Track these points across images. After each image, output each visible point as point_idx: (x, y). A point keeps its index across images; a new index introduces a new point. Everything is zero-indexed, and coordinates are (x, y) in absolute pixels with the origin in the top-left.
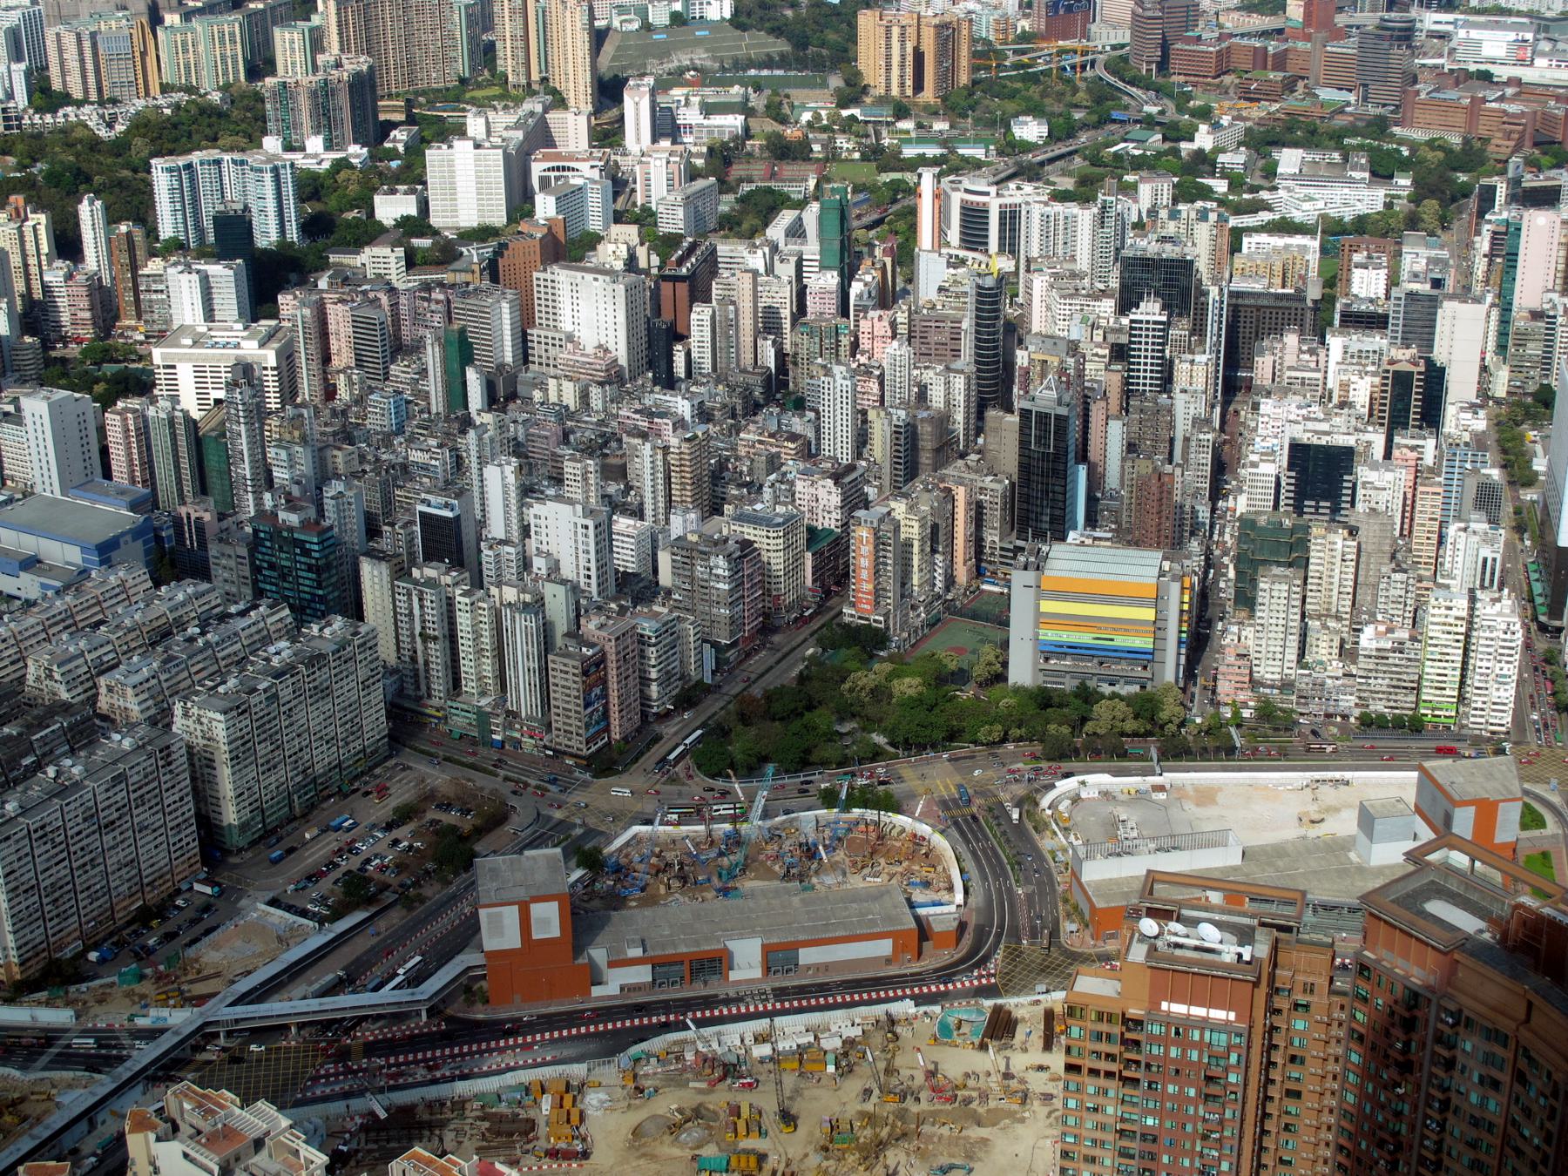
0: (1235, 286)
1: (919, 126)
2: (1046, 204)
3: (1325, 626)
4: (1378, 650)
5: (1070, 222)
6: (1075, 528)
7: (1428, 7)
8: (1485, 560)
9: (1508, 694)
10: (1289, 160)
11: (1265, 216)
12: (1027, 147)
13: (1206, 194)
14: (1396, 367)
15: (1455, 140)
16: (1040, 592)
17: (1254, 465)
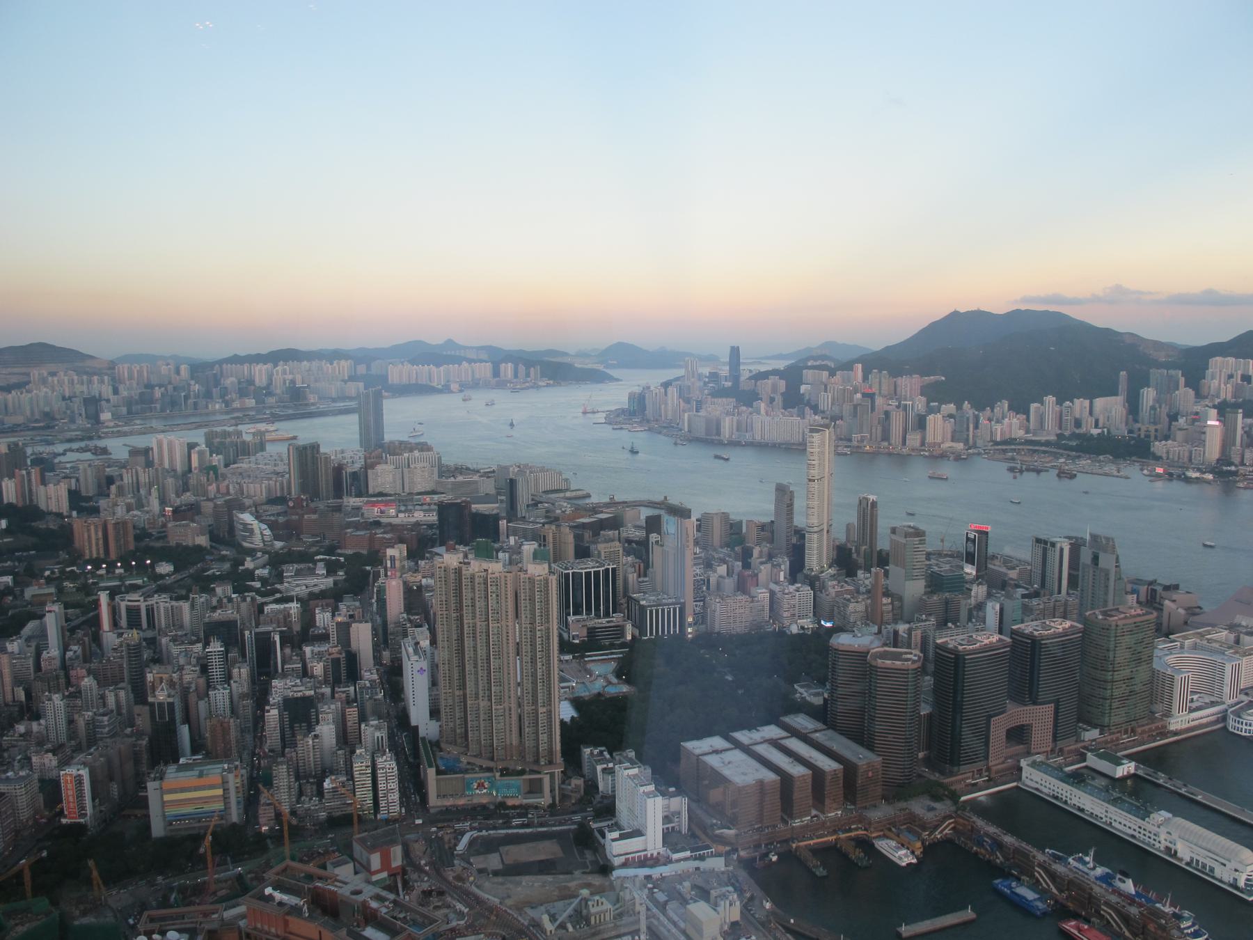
0: (258, 630)
1: (108, 572)
2: (166, 602)
3: (308, 782)
4: (333, 788)
6: (183, 756)
7: (351, 496)
8: (378, 737)
9: (395, 796)
10: (289, 570)
11: (278, 595)
12: (162, 577)
13: (251, 589)
14: (332, 656)
15: (365, 552)
16: (163, 792)
17: (268, 711)
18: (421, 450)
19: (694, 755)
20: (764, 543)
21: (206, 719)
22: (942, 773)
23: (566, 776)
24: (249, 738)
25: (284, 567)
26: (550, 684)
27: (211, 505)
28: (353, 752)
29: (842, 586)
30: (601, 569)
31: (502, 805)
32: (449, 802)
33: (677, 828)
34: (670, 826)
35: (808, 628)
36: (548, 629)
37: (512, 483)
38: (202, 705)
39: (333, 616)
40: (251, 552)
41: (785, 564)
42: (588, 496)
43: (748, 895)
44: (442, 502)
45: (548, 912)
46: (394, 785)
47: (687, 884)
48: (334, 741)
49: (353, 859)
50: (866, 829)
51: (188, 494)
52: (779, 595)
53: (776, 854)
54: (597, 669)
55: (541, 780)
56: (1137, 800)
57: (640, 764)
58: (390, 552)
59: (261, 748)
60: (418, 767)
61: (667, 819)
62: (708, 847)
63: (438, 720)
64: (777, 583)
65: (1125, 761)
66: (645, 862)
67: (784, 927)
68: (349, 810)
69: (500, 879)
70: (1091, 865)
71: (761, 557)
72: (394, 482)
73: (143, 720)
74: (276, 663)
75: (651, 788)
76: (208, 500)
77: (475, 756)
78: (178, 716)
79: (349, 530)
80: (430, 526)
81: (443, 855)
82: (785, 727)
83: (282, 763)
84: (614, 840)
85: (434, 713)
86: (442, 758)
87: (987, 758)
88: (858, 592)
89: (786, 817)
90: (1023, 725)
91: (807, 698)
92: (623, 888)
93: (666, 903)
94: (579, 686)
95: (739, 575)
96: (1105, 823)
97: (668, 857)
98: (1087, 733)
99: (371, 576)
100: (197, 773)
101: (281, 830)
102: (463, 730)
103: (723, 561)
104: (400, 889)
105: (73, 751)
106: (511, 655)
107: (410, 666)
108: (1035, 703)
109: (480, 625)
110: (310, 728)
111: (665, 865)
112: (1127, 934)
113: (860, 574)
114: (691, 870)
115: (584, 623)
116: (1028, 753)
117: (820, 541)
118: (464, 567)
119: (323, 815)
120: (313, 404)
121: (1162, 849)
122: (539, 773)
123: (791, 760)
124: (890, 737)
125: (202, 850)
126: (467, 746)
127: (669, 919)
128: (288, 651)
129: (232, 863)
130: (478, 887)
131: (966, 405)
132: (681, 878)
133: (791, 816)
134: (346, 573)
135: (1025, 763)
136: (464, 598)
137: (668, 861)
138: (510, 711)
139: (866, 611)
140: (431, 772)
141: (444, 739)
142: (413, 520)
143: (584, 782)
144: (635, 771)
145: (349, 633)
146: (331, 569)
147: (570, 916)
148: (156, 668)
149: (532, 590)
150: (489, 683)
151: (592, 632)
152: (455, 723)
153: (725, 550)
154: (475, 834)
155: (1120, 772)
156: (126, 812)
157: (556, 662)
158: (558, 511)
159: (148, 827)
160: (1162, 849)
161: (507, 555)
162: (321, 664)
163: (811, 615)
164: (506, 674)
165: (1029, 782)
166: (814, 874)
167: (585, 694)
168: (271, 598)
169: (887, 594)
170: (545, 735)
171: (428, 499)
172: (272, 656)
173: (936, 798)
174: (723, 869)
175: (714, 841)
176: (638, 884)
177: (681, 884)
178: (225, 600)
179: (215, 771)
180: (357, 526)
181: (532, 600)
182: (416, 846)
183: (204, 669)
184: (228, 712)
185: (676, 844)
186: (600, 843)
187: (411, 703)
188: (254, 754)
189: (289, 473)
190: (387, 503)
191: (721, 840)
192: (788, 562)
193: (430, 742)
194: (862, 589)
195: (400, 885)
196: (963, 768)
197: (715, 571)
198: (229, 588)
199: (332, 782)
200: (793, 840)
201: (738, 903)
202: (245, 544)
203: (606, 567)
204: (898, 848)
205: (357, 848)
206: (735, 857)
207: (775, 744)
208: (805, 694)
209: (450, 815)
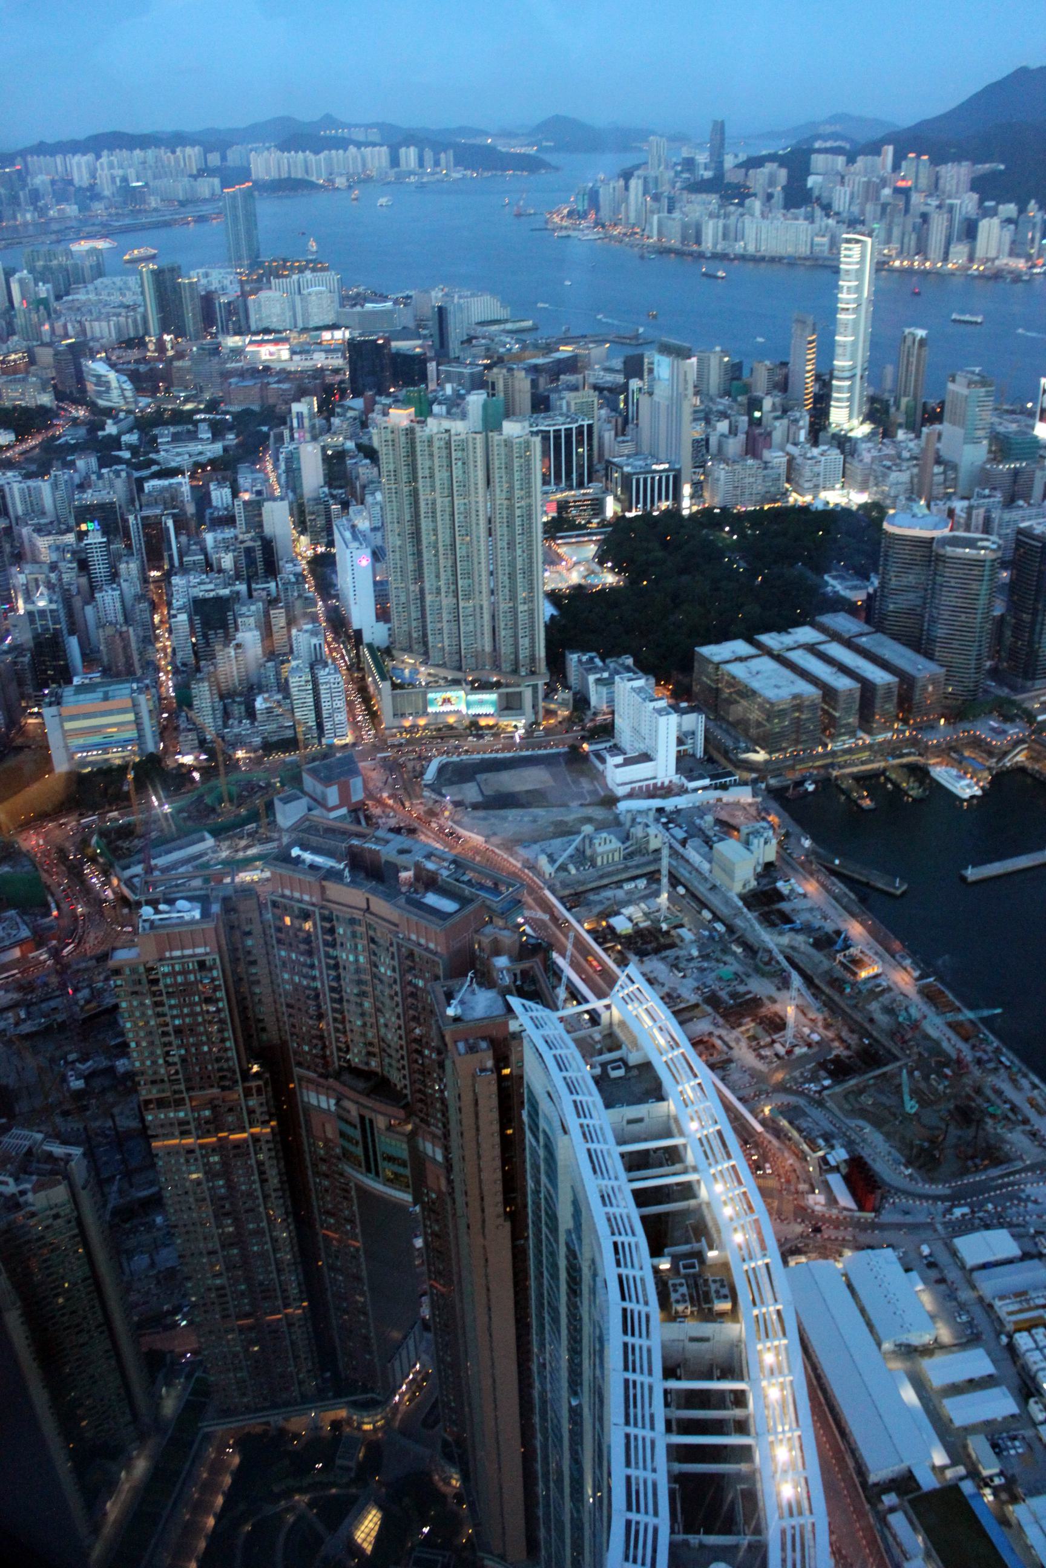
0: (145, 513)
5: (39, 490)
7: (228, 333)
10: (164, 435)
11: (155, 468)
13: (119, 460)
15: (256, 408)
16: (62, 719)
18: (314, 270)
19: (711, 662)
20: (776, 392)
21: (98, 628)
22: (1014, 689)
23: (550, 690)
25: (156, 431)
27: (49, 351)
29: (880, 450)
30: (574, 426)
31: (474, 727)
33: (691, 751)
34: (682, 748)
35: (837, 505)
36: (530, 505)
37: (441, 312)
38: (89, 609)
39: (235, 494)
40: (109, 412)
41: (805, 421)
42: (534, 329)
43: (783, 831)
44: (352, 339)
45: (543, 851)
46: (340, 703)
47: (709, 818)
48: (259, 651)
50: (920, 755)
51: (15, 338)
52: (799, 460)
53: (814, 782)
55: (520, 693)
57: (640, 674)
58: (296, 407)
60: (363, 679)
61: (680, 742)
62: (730, 774)
64: (796, 444)
67: (826, 868)
68: (289, 734)
69: (481, 813)
71: (774, 408)
72: (283, 313)
74: (171, 557)
76: (43, 344)
77: (438, 666)
79: (233, 380)
80: (336, 371)
82: (822, 629)
83: (202, 680)
84: (617, 766)
85: (383, 615)
86: (394, 668)
88: (899, 456)
91: (842, 593)
94: (554, 575)
95: (747, 433)
99: (272, 439)
100: (101, 695)
103: (724, 415)
106: (482, 539)
107: (348, 555)
109: (441, 502)
111: (679, 795)
113: (901, 435)
114: (712, 802)
115: (552, 497)
117: (851, 389)
118: (418, 428)
119: (257, 740)
120: (156, 210)
123: (834, 670)
125: (125, 788)
126: (426, 653)
128: (184, 539)
131: (1032, 204)
132: (701, 810)
133: (833, 737)
134: (237, 436)
136: (419, 466)
137: (683, 791)
138: (481, 608)
139: (912, 482)
141: (398, 646)
142: (309, 364)
143: (575, 694)
144: (640, 683)
145: (260, 515)
146: (218, 430)
147: (571, 856)
148: (28, 568)
149: (509, 456)
150: (455, 574)
151: (563, 506)
152: (410, 626)
153: (726, 401)
158: (502, 350)
161: (444, 408)
162: (231, 555)
163: (838, 486)
166: (859, 806)
167: (563, 586)
168: (145, 473)
169: (939, 461)
170: (527, 640)
171: (326, 335)
172: (164, 546)
173: (1008, 718)
174: (750, 800)
175: (737, 767)
177: (702, 818)
178: (94, 477)
179: (123, 692)
180: (242, 374)
181: (509, 468)
183: (84, 565)
184: (121, 619)
185: (691, 771)
186: (596, 768)
187: (352, 602)
189: (145, 306)
190: (276, 342)
191: (749, 766)
192: (807, 418)
193: (379, 649)
194: (906, 454)
196: (1038, 683)
197: (715, 429)
198: (93, 461)
199: (265, 700)
200: (832, 765)
201: (774, 842)
202: (102, 403)
203: (580, 423)
204: (961, 778)
205: (308, 781)
206: (763, 786)
207: (812, 649)
209: (413, 739)
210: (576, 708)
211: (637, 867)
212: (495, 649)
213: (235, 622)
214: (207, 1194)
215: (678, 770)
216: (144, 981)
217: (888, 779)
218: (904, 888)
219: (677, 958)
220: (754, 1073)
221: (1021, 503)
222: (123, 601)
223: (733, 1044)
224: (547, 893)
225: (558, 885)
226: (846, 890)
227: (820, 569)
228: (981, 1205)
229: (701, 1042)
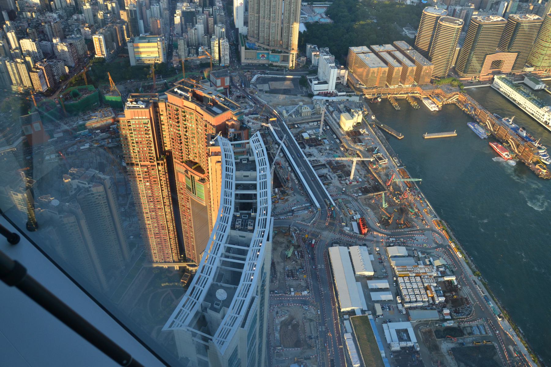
3: (192, 48)
17: (176, 17)
24: (168, 27)
26: (296, 15)
28: (211, 37)
31: (271, 65)
32: (250, 61)
33: (342, 83)
38: (148, 11)
46: (227, 52)
47: (342, 105)
48: (203, 32)
49: (210, 81)
50: (420, 94)
53: (381, 98)
54: (317, 10)
55: (288, 57)
56: (540, 100)
59: (173, 32)
61: (338, 78)
62: (353, 92)
63: (247, 26)
65: (541, 83)
66: (326, 94)
67: (378, 127)
68: (209, 61)
69: (268, 94)
70: (511, 123)
73: (124, 16)
75: (334, 65)
77: (262, 43)
78: (138, 16)
81: (246, 83)
83: (181, 39)
84: (315, 84)
85: (246, 23)
87: (480, 72)
89: (388, 84)
90: (500, 61)
91: (408, 35)
92: (316, 104)
93: (333, 111)
96: (523, 107)
97: (336, 94)
98: (528, 68)
100: (147, 41)
101: (181, 67)
102: (257, 32)
104: (228, 94)
105: (97, 28)
108: (508, 52)
110: (193, 26)
112: (516, 151)
116: (499, 73)
119: (198, 62)
121: (543, 121)
122: (288, 53)
124: (440, 57)
126: (259, 39)
127: (333, 118)
129: (163, 78)
130: (258, 96)
132: (340, 103)
133: (390, 84)
135: (497, 77)
137: (336, 95)
140: (243, 48)
141: (249, 35)
147: (294, 112)
150: (270, 12)
154: (259, 75)
155: (537, 87)
156: (120, 55)
157: (300, 5)
159: (129, 61)
160: (543, 121)
164: (277, 8)
165: (496, 85)
167: (311, 21)
174: (358, 101)
175: (356, 90)
176: (322, 103)
177: (340, 105)
182: (235, 78)
184: (159, 16)
188: (170, 35)
193: (243, 35)
195: (228, 93)
204: (432, 104)
205: (212, 77)
207: (389, 53)
208: (407, 33)
209: (250, 68)
210: (306, 64)
211: (315, 118)
212: (281, 40)
213: (196, 20)
214: (145, 195)
215: (336, 88)
216: (127, 125)
217: (407, 101)
218: (403, 137)
219: (321, 149)
220: (337, 188)
221: (481, 10)
222: (160, 9)
223: (333, 178)
224: (284, 122)
225: (288, 121)
226: (383, 135)
227: (403, 26)
228: (399, 239)
229: (323, 176)
